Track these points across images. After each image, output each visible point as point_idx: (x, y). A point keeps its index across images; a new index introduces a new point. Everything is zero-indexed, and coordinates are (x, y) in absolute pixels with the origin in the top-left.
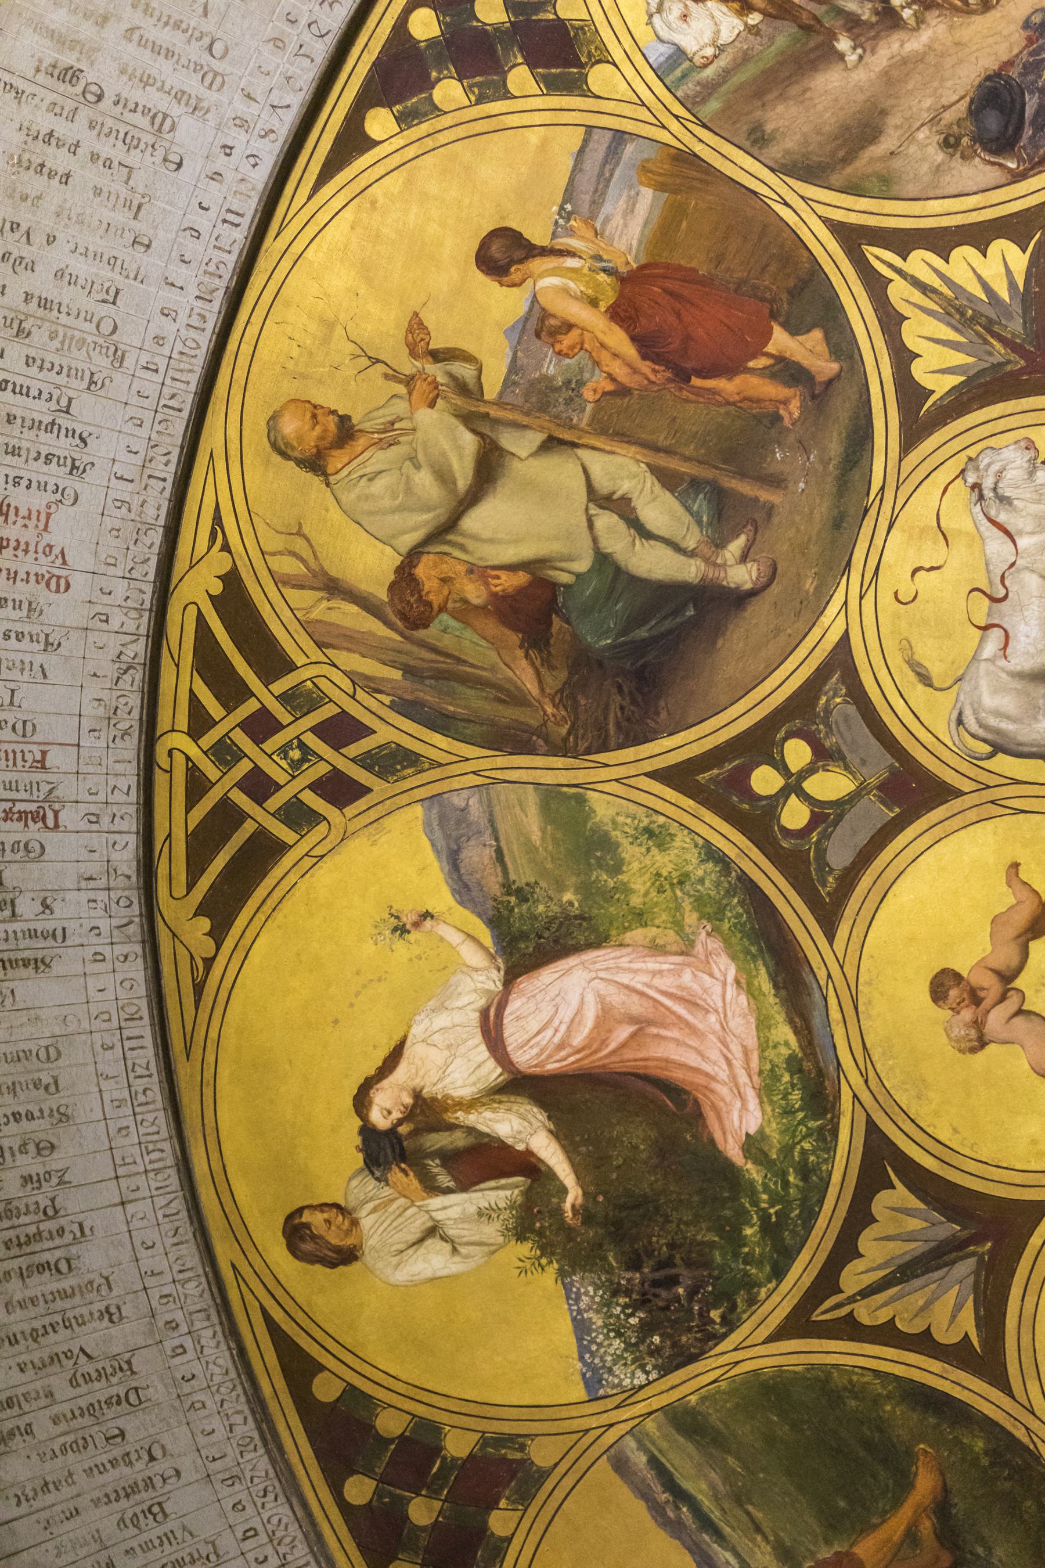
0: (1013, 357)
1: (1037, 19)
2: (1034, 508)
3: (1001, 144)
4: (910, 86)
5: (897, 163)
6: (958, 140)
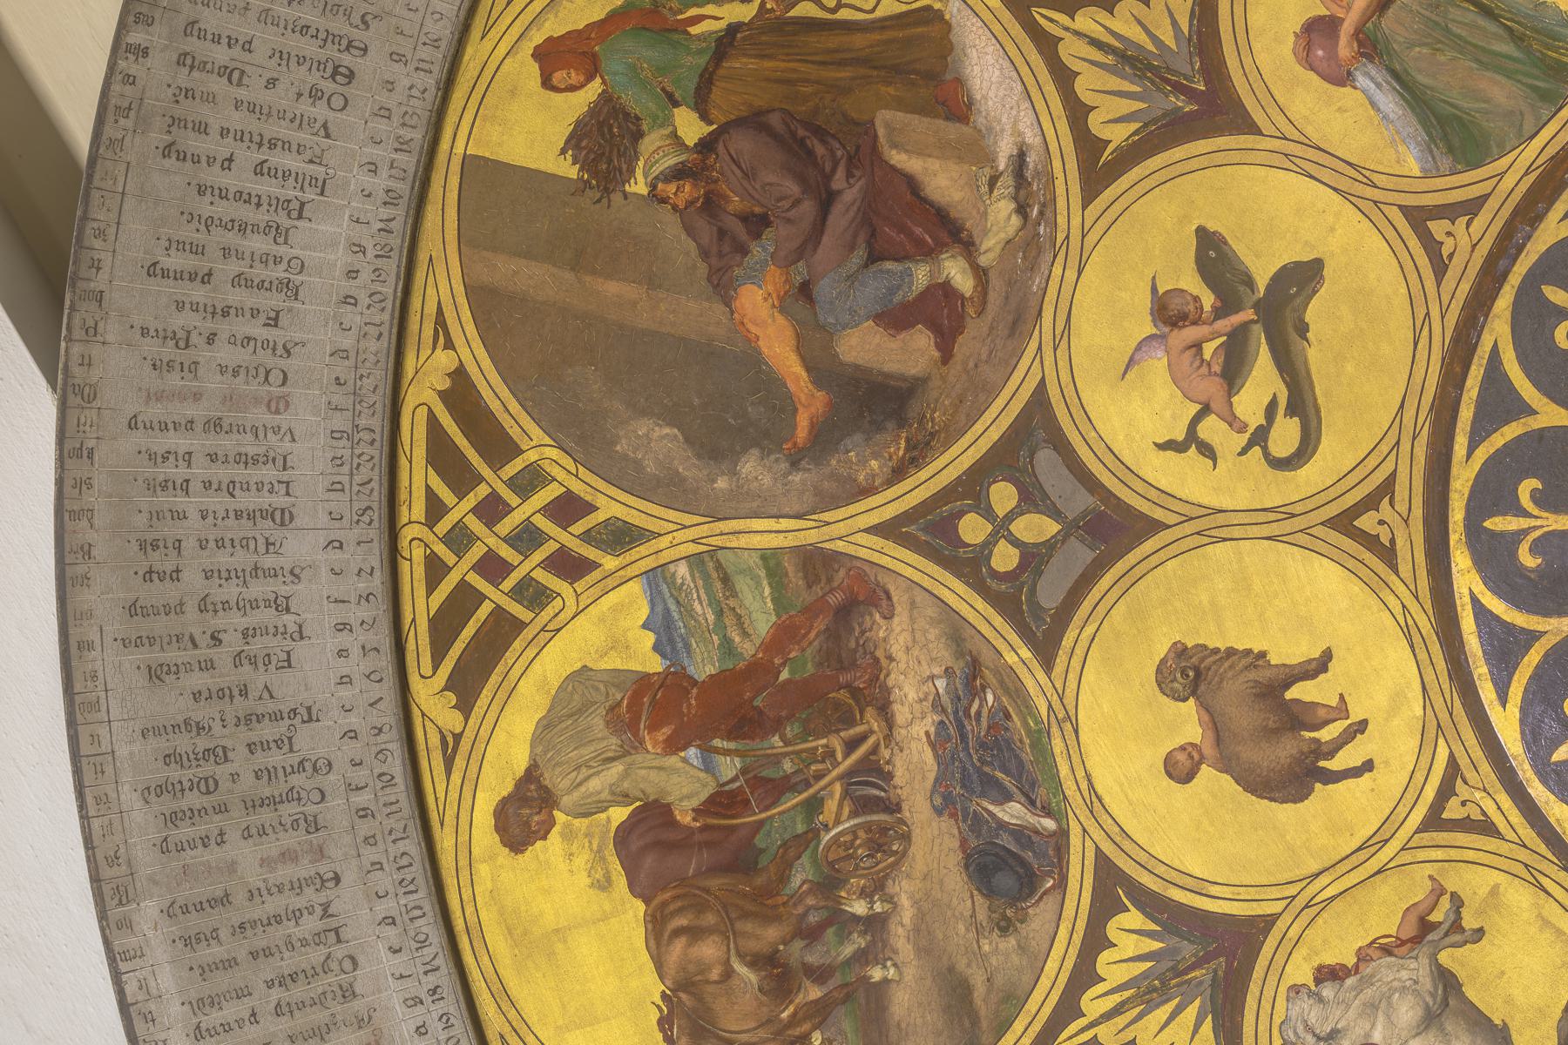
0: (1213, 965)
1: (938, 801)
2: (1351, 1013)
3: (1028, 884)
4: (940, 936)
5: (999, 980)
6: (1008, 920)
